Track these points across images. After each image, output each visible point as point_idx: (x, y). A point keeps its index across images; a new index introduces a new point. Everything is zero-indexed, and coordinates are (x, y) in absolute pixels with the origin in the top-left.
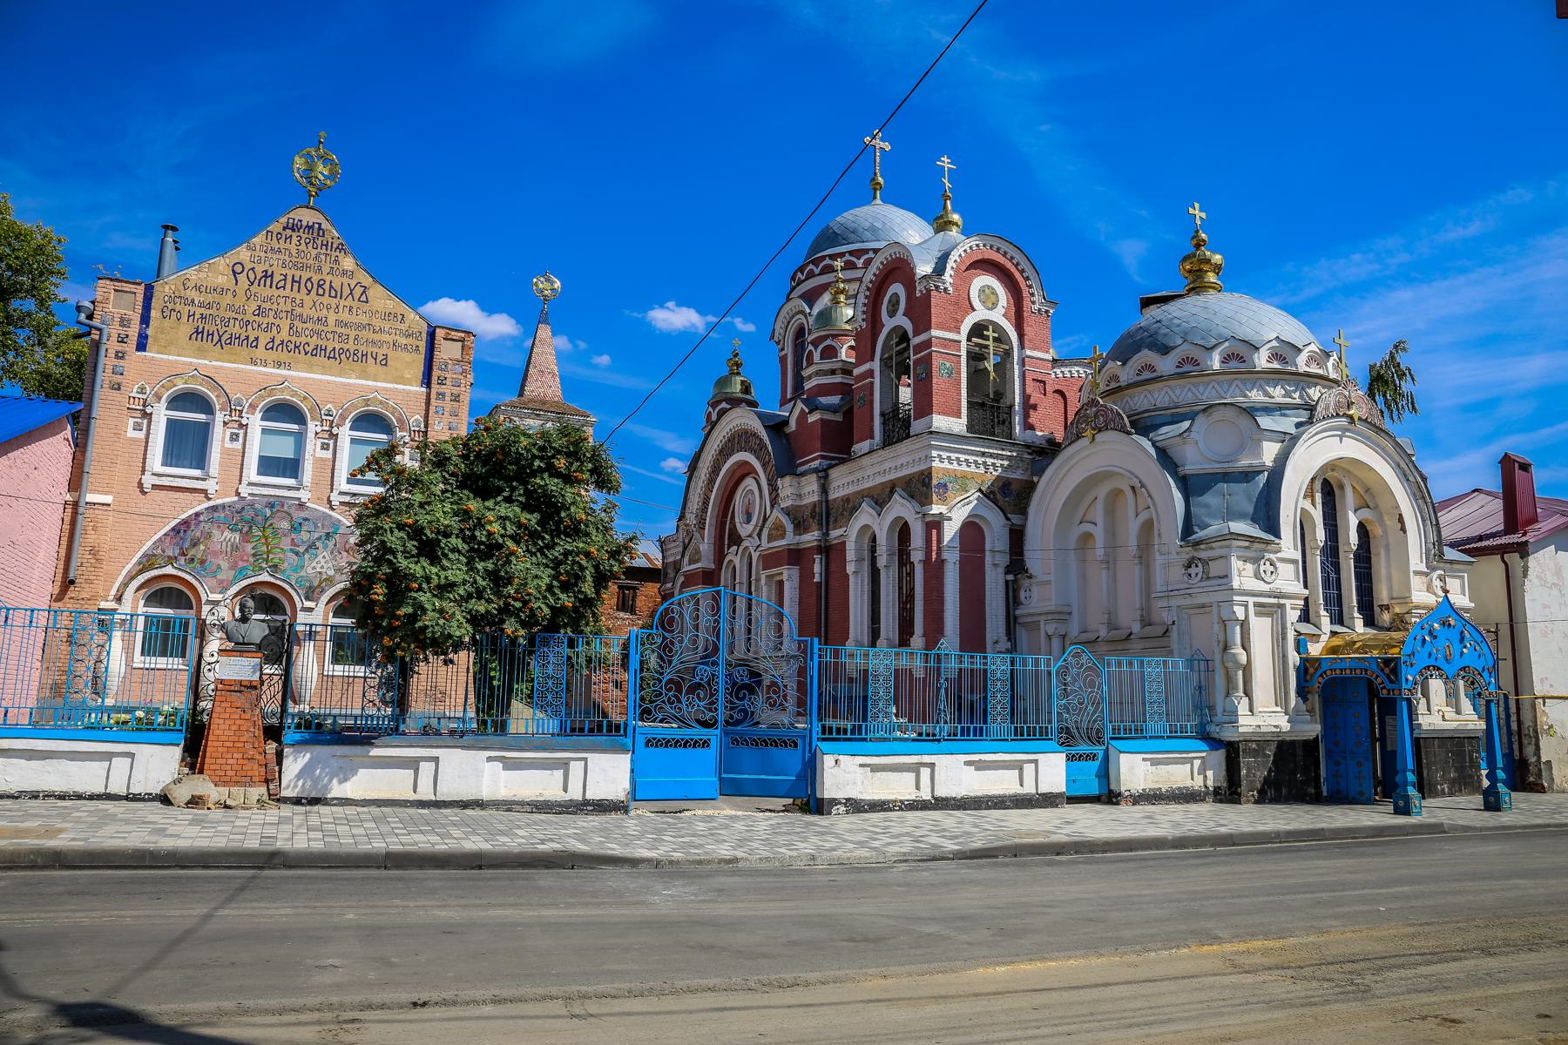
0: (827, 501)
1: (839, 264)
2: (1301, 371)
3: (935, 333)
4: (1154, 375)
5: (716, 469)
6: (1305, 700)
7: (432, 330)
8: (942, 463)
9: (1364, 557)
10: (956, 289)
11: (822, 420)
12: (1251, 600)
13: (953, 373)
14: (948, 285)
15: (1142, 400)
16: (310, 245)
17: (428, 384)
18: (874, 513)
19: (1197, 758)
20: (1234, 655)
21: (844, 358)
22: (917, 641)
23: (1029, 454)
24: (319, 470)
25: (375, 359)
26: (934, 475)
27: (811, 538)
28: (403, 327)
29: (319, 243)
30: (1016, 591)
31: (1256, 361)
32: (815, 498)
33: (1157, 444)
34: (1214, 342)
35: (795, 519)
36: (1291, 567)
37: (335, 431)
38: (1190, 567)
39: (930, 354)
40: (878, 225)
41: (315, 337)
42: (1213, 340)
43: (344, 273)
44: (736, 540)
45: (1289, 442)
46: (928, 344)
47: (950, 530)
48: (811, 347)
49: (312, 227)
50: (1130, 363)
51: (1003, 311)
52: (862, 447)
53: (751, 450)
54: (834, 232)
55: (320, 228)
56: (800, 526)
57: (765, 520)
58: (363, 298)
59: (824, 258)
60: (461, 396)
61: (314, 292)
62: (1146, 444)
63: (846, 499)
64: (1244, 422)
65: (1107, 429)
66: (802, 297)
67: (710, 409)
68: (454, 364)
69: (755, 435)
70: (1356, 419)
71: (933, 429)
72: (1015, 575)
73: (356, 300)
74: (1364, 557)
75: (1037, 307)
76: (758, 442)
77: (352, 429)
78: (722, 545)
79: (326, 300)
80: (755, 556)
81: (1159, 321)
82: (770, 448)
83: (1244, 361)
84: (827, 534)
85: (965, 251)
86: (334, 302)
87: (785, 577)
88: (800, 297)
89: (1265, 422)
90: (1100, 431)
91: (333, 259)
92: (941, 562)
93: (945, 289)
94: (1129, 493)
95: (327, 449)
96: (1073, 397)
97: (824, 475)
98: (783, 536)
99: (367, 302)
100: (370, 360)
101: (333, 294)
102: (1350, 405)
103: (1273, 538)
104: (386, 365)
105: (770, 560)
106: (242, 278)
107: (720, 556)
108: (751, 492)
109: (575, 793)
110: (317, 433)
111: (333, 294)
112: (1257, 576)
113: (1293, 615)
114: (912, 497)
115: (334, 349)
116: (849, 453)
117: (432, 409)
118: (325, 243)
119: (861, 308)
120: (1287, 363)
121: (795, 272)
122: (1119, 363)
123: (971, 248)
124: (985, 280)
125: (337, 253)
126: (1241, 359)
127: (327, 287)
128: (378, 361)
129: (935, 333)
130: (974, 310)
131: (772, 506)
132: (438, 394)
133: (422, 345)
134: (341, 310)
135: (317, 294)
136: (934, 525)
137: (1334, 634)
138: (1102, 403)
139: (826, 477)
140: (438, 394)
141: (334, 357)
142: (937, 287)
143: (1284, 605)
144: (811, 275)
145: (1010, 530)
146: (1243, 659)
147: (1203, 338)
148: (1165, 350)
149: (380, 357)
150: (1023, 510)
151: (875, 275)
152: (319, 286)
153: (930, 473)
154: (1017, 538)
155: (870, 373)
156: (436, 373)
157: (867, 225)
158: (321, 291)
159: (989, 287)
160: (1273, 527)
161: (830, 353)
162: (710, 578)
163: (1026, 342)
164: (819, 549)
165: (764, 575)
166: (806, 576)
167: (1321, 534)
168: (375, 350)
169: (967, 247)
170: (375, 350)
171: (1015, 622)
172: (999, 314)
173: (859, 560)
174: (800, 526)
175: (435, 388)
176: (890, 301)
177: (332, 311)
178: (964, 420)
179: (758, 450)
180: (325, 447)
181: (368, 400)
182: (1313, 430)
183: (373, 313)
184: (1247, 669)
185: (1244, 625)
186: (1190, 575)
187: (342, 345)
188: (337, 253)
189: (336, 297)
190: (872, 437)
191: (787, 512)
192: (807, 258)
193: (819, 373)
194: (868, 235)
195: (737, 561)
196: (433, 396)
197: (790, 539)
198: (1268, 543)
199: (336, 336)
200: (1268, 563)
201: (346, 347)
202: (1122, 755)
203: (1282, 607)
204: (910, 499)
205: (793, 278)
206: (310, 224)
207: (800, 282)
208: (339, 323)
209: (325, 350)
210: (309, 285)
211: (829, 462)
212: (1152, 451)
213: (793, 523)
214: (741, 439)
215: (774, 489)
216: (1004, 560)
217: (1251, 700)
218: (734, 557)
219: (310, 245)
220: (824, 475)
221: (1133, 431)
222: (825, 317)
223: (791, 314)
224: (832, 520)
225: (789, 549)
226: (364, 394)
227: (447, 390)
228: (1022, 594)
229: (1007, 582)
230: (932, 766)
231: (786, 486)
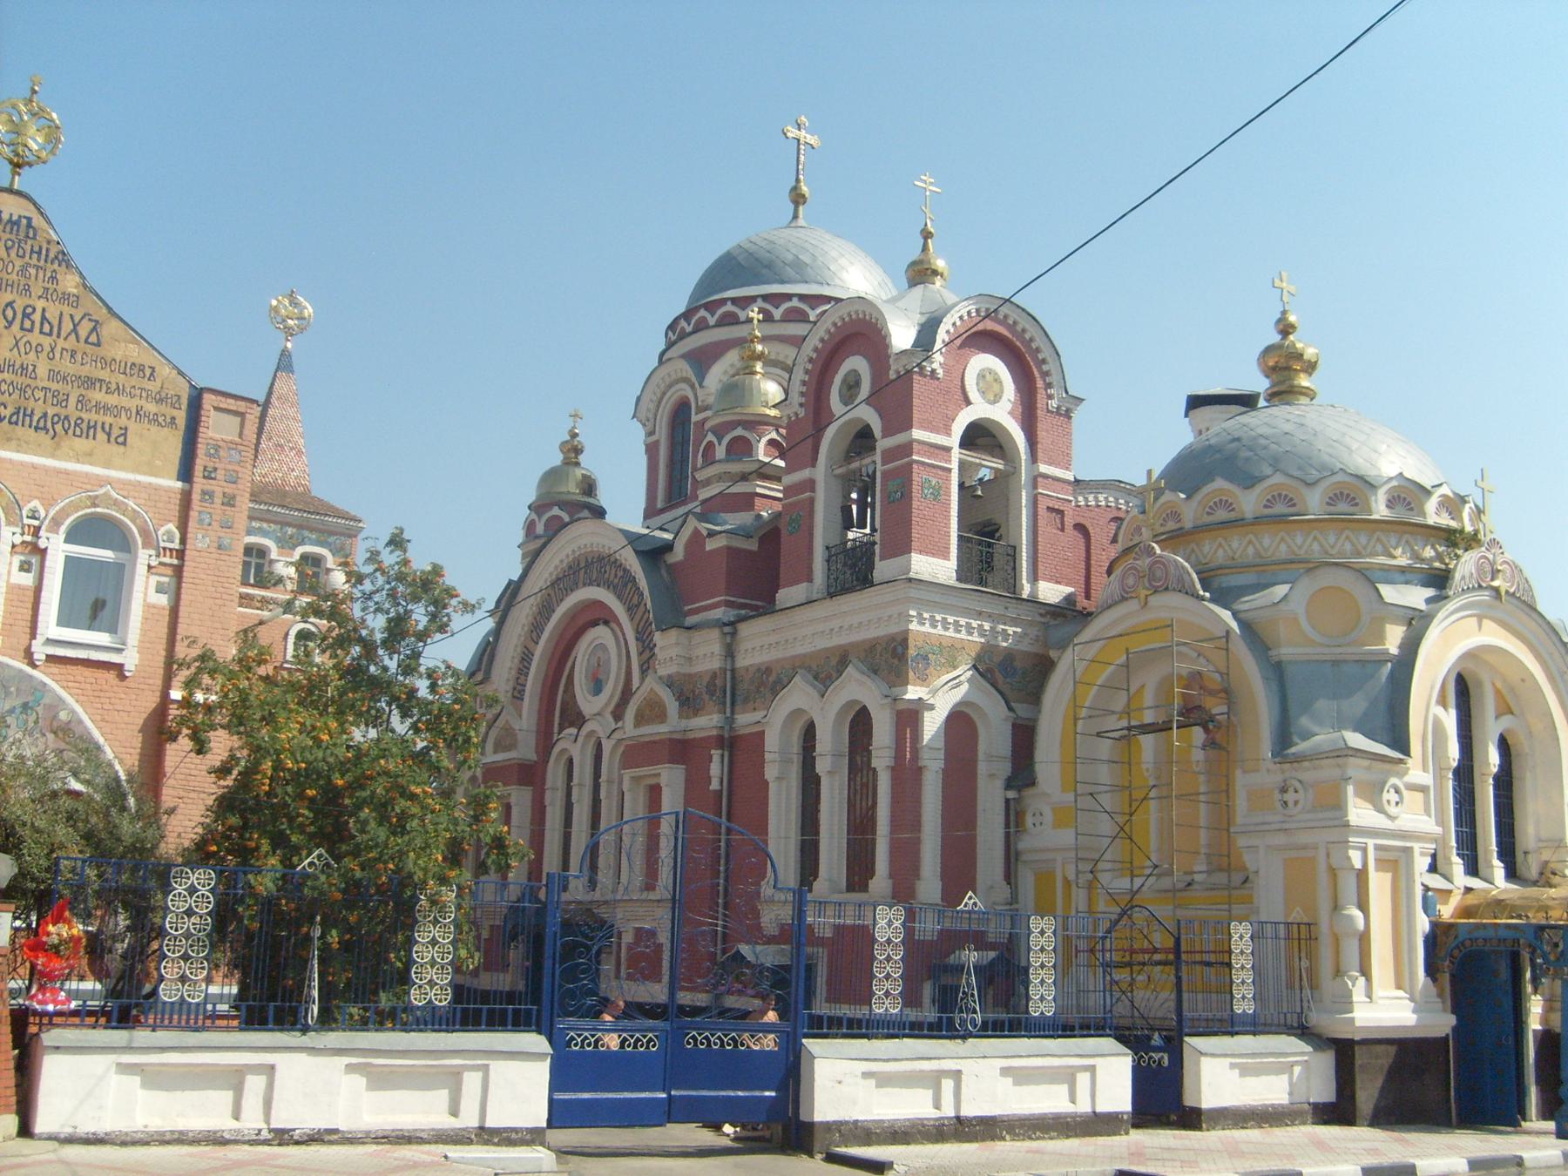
0: (733, 670)
1: (755, 314)
2: (1430, 522)
3: (917, 434)
4: (1232, 516)
5: (546, 610)
6: (1434, 980)
7: (195, 393)
8: (922, 628)
9: (1505, 782)
10: (947, 371)
11: (729, 549)
12: (1371, 843)
13: (939, 494)
14: (935, 366)
15: (1215, 550)
16: (13, 253)
17: (186, 473)
18: (816, 694)
19: (1297, 1063)
20: (1350, 917)
21: (761, 458)
22: (880, 881)
23: (1041, 615)
24: (15, 603)
25: (109, 435)
26: (911, 642)
27: (707, 723)
28: (150, 386)
29: (28, 248)
30: (1020, 816)
31: (1373, 505)
32: (716, 664)
33: (1242, 616)
34: (1315, 474)
35: (681, 694)
36: (1419, 796)
37: (42, 544)
39: (910, 464)
40: (805, 258)
41: (15, 396)
42: (1314, 472)
43: (65, 298)
44: (574, 718)
45: (1417, 624)
46: (906, 449)
47: (932, 724)
48: (710, 437)
49: (17, 223)
50: (1198, 497)
51: (1009, 406)
52: (786, 596)
53: (608, 585)
54: (740, 264)
55: (29, 226)
56: (689, 703)
57: (627, 694)
58: (93, 338)
59: (723, 302)
60: (238, 498)
61: (16, 327)
62: (1226, 615)
63: (767, 670)
64: (1358, 589)
66: (689, 356)
67: (534, 516)
68: (229, 449)
69: (618, 565)
70: (1503, 594)
71: (912, 575)
72: (1019, 791)
73: (82, 339)
74: (1505, 782)
75: (1054, 403)
76: (620, 574)
77: (67, 541)
78: (550, 723)
79: (35, 338)
80: (607, 746)
81: (1238, 439)
82: (643, 583)
83: (1356, 504)
84: (731, 720)
85: (961, 318)
86: (46, 341)
87: (663, 781)
88: (683, 356)
89: (1390, 593)
90: (1155, 592)
91: (49, 274)
92: (919, 771)
93: (933, 371)
95: (28, 571)
96: (1101, 533)
97: (730, 629)
98: (662, 717)
99: (98, 344)
100: (101, 436)
101: (47, 328)
102: (1495, 573)
103: (1401, 756)
104: (124, 443)
105: (637, 754)
107: (546, 743)
108: (603, 647)
109: (469, 1119)
110: (14, 546)
111: (47, 328)
112: (1381, 810)
113: (1422, 863)
114: (875, 672)
115: (45, 415)
116: (772, 601)
117: (193, 514)
118: (36, 249)
119: (797, 387)
120: (1412, 509)
121: (676, 321)
122: (1183, 496)
123: (969, 313)
124: (985, 362)
125: (56, 266)
126: (1353, 501)
127: (37, 317)
128: (112, 439)
129: (917, 434)
130: (968, 402)
131: (645, 669)
132: (204, 493)
133: (181, 416)
134: (58, 355)
135: (22, 329)
136: (910, 717)
137: (1468, 890)
138: (1158, 551)
139: (734, 634)
140: (204, 493)
141: (45, 428)
142: (922, 368)
143: (1411, 848)
144: (702, 326)
145: (1014, 725)
146: (1361, 925)
147: (1300, 468)
148: (1249, 481)
149: (116, 432)
150: (1035, 697)
151: (822, 340)
152: (26, 315)
153: (905, 640)
154: (1024, 738)
155: (810, 485)
156: (201, 462)
157: (790, 257)
158: (27, 324)
159: (990, 371)
160: (1402, 745)
161: (741, 448)
162: (530, 774)
163: (1040, 454)
164: (720, 742)
165: (628, 774)
166: (695, 784)
167: (1453, 751)
168: (109, 420)
169: (964, 312)
170: (109, 420)
171: (1017, 860)
172: (1003, 413)
173: (785, 761)
174: (689, 703)
175: (199, 483)
176: (844, 381)
177: (43, 355)
178: (952, 564)
179: (623, 584)
180: (25, 567)
181: (97, 497)
182: (1451, 606)
183: (107, 363)
184: (1364, 938)
185: (1362, 875)
186: (1285, 803)
187: (56, 410)
188: (56, 266)
189: (50, 334)
190: (810, 580)
191: (670, 682)
192: (695, 296)
193: (720, 478)
195: (575, 751)
196: (196, 496)
197: (673, 724)
198: (1401, 761)
199: (49, 395)
200: (1392, 791)
201: (63, 412)
202: (1204, 1060)
203: (1408, 851)
204: (873, 675)
205: (672, 327)
206: (15, 218)
207: (683, 335)
208: (53, 375)
209: (31, 416)
210: (9, 313)
211: (736, 612)
212: (1234, 625)
213: (678, 699)
214: (594, 567)
215: (647, 647)
216: (1005, 769)
217: (1369, 980)
218: (570, 744)
219: (13, 253)
220: (730, 629)
221: (1207, 595)
222: (736, 390)
223: (668, 381)
224: (739, 699)
225: (670, 740)
226: (89, 487)
227: (218, 487)
228: (1029, 820)
229: (1007, 801)
230: (957, 1075)
231: (667, 644)
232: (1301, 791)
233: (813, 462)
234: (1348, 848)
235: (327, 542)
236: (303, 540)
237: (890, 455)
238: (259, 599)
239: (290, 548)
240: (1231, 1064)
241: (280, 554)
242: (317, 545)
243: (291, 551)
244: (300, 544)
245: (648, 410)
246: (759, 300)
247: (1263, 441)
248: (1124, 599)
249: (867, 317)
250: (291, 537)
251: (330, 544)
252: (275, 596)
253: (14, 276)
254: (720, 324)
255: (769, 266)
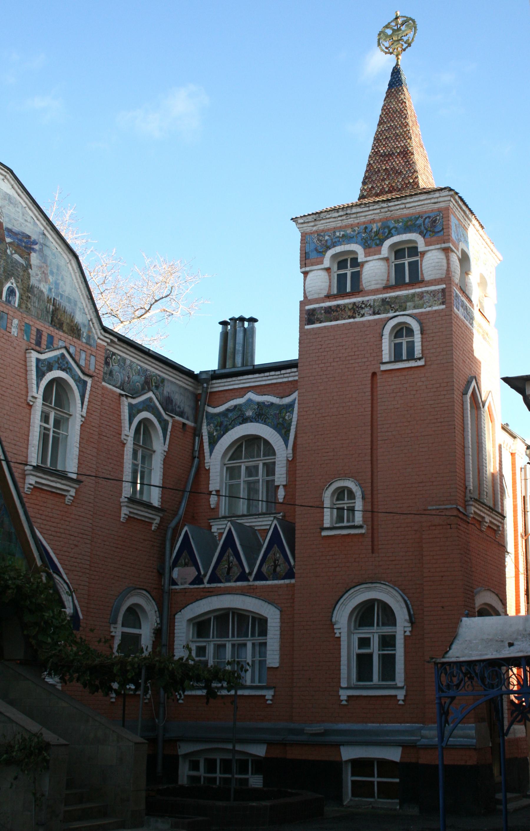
235: (415, 225)
236: (390, 232)
238: (350, 307)
239: (377, 245)
241: (367, 255)
242: (405, 233)
243: (377, 248)
244: (387, 238)
250: (377, 233)
251: (420, 226)
252: (366, 299)
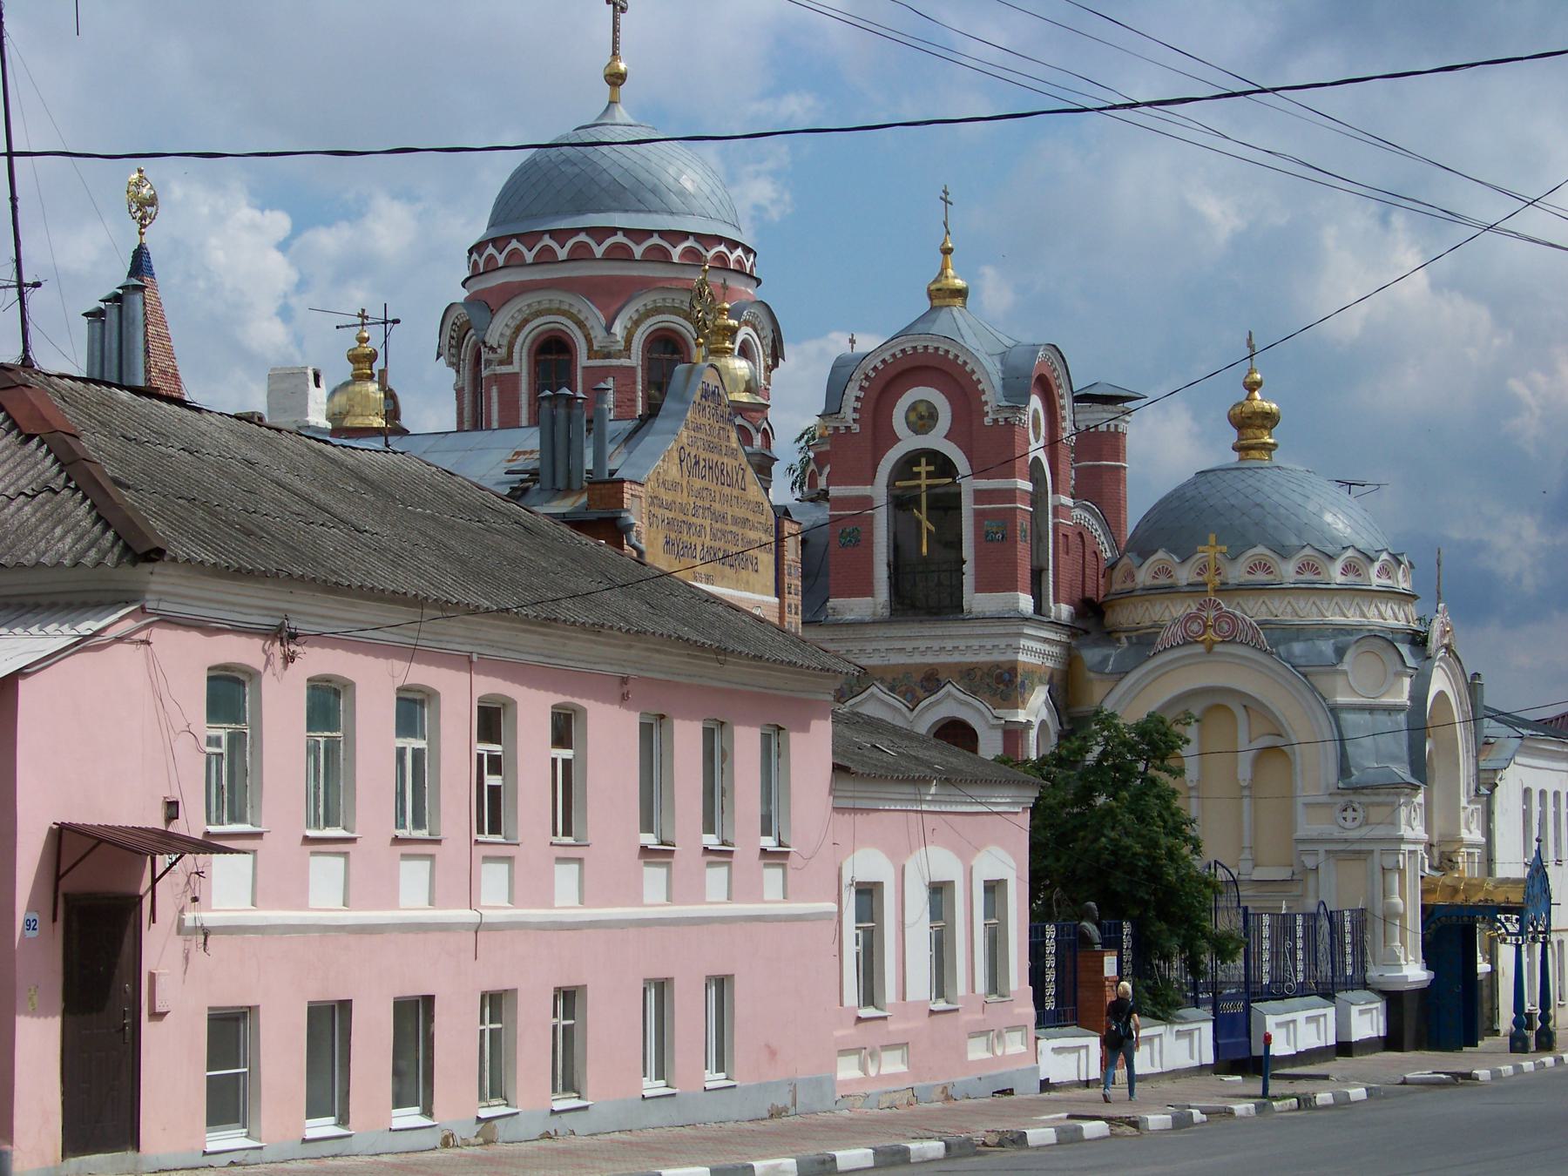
17: (779, 592)
38: (1345, 810)
65: (1232, 642)
94: (1241, 714)
99: (744, 490)
103: (1417, 783)
104: (757, 571)
106: (684, 464)
176: (913, 407)
185: (1402, 872)
194: (675, 201)
232: (1360, 810)
233: (871, 480)
234: (1398, 854)
237: (980, 496)
240: (1360, 1011)
245: (502, 335)
246: (656, 235)
247: (1282, 511)
248: (1186, 643)
249: (951, 356)
253: (717, 440)
254: (609, 256)
255: (654, 191)
